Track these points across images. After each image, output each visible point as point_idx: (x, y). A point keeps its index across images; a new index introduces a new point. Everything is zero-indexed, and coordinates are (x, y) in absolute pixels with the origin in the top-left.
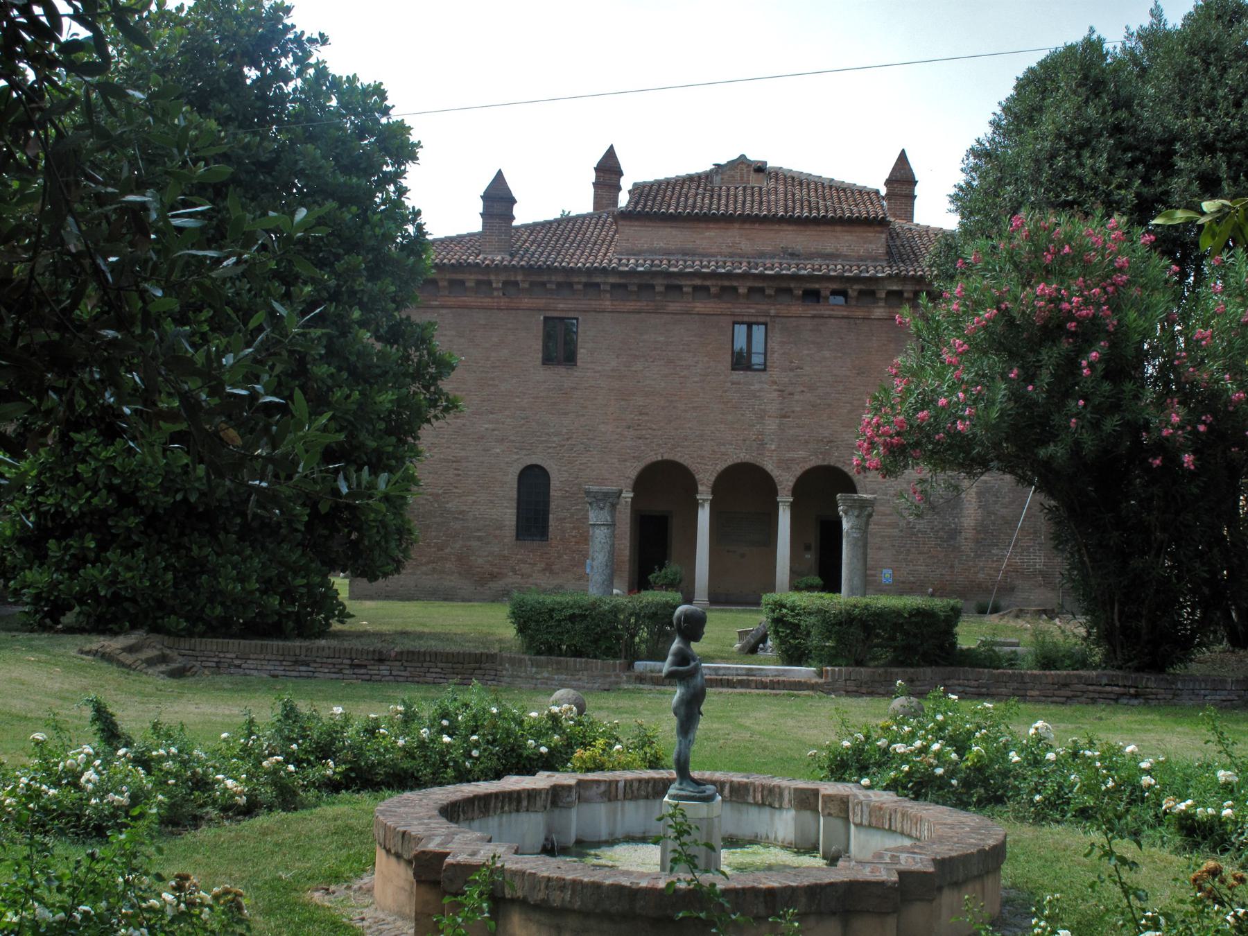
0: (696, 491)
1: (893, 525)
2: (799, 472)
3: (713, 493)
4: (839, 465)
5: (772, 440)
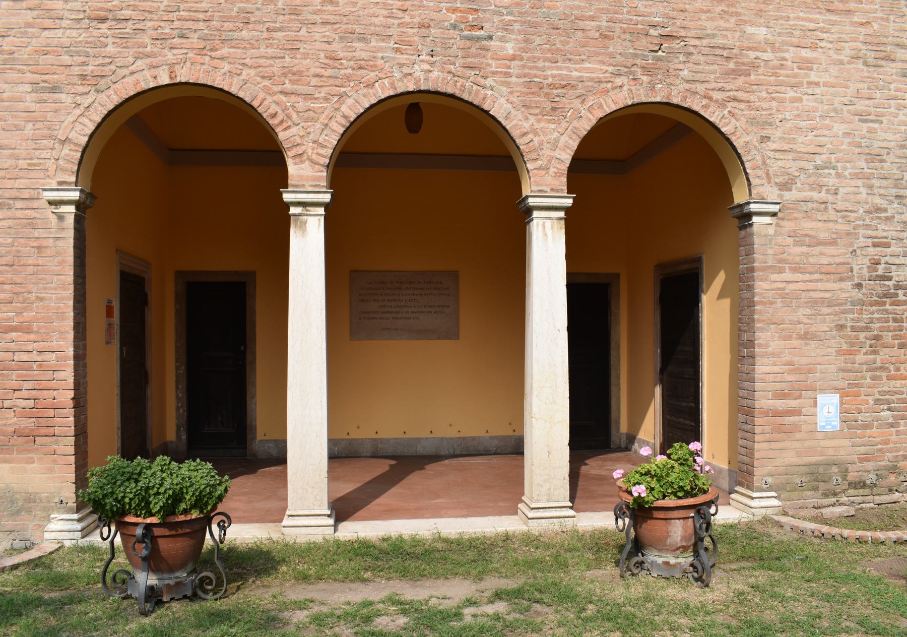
0: (282, 179)
1: (843, 273)
2: (585, 126)
3: (334, 183)
4: (696, 105)
5: (506, 27)
